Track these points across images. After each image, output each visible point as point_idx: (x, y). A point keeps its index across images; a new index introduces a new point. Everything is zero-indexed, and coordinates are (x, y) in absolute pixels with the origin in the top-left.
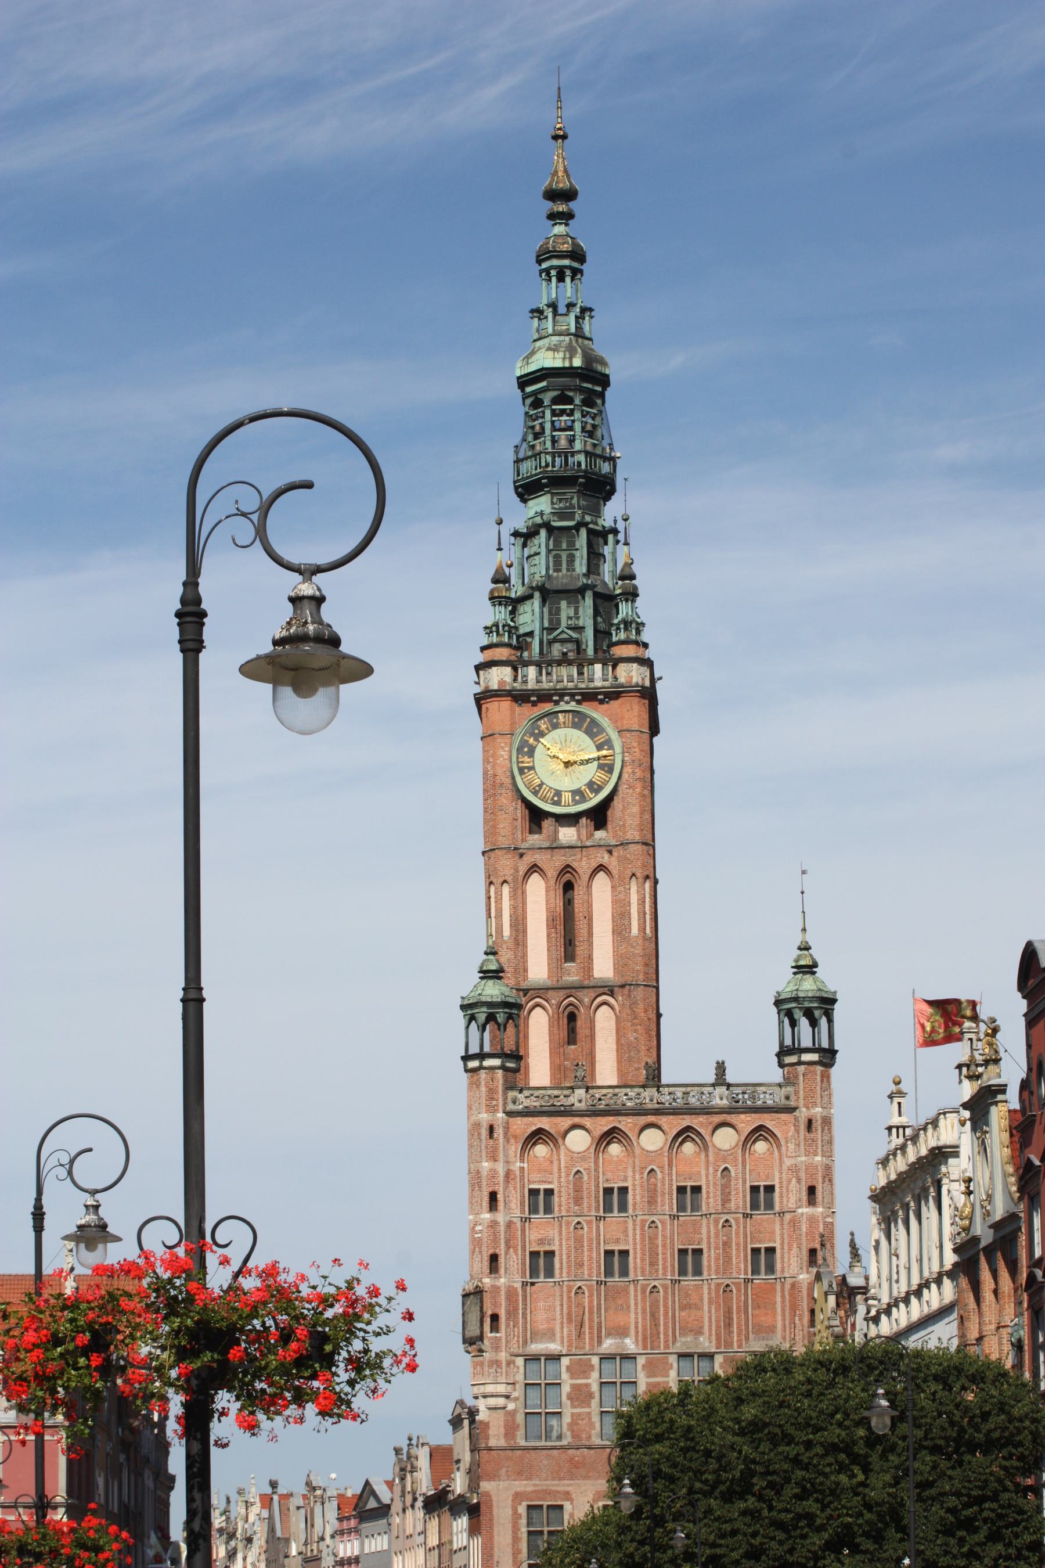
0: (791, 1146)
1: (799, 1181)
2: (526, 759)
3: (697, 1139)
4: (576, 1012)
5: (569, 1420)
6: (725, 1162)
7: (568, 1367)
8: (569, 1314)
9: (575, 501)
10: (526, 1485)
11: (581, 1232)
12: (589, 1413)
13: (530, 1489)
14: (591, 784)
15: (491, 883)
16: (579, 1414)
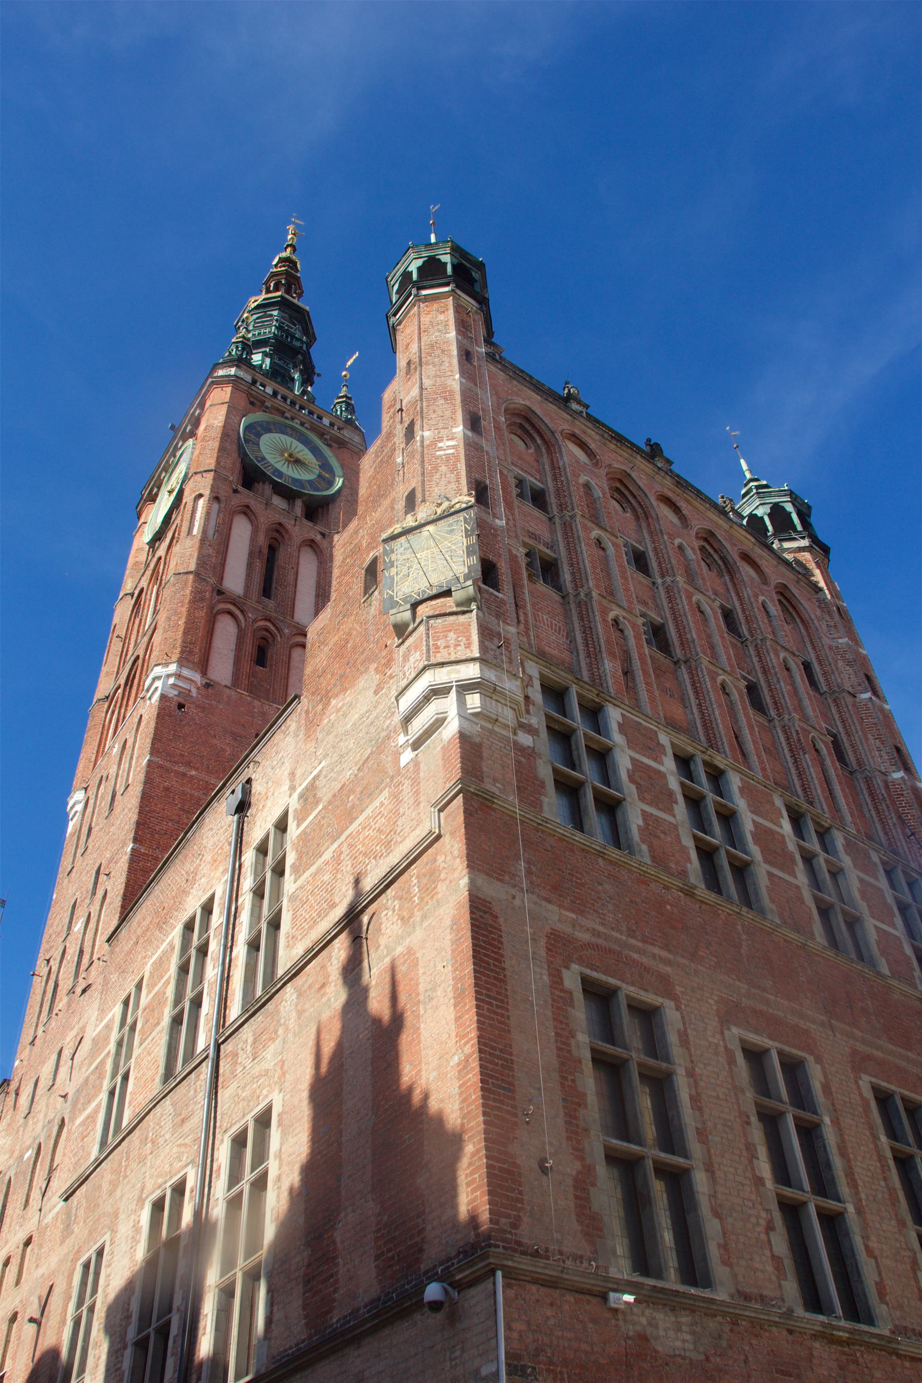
0: (824, 627)
1: (849, 663)
2: (253, 436)
3: (715, 556)
4: (270, 640)
5: (640, 822)
6: (763, 595)
7: (620, 726)
8: (608, 642)
9: (291, 366)
10: (574, 924)
11: (601, 553)
12: (676, 827)
13: (585, 937)
14: (310, 482)
15: (201, 496)
16: (657, 819)
